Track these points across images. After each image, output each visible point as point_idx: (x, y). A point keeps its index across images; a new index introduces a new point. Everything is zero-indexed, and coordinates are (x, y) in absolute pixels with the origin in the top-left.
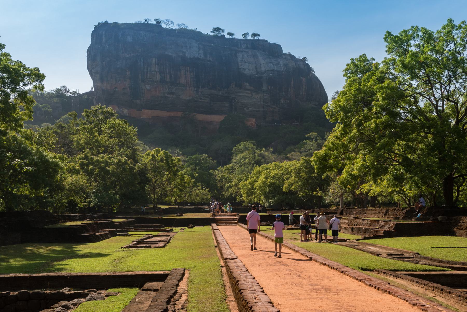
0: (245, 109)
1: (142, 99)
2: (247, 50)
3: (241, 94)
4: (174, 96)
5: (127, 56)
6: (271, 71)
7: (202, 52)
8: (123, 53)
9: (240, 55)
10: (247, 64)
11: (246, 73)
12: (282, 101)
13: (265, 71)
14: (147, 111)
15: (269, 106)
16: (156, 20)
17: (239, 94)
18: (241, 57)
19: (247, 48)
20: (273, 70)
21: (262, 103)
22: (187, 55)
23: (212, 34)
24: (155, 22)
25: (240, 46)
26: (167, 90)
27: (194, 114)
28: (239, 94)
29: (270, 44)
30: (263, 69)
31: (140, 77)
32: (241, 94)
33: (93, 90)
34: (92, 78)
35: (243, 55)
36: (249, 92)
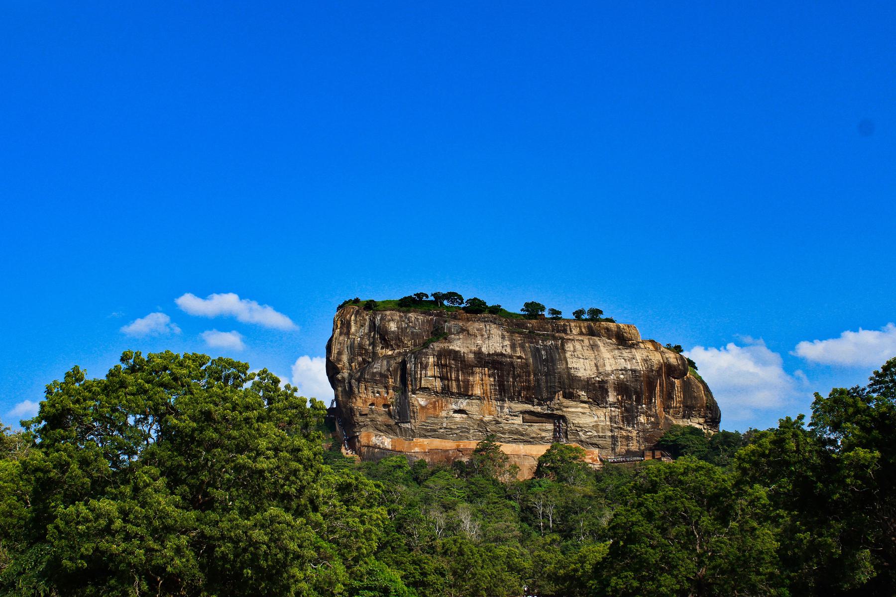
0: (581, 433)
1: (413, 421)
2: (580, 338)
3: (573, 410)
4: (464, 416)
5: (390, 353)
6: (621, 370)
7: (507, 343)
8: (382, 348)
9: (569, 347)
10: (582, 360)
11: (579, 374)
12: (642, 419)
13: (612, 372)
14: (421, 440)
15: (621, 428)
16: (434, 295)
17: (570, 410)
18: (572, 349)
19: (581, 333)
20: (625, 370)
21: (608, 423)
22: (484, 350)
23: (522, 313)
24: (432, 298)
25: (569, 332)
26: (454, 407)
27: (498, 444)
28: (570, 410)
29: (618, 327)
30: (608, 368)
31: (410, 387)
32: (573, 410)
33: (335, 406)
34: (333, 387)
35: (574, 347)
36: (587, 406)
